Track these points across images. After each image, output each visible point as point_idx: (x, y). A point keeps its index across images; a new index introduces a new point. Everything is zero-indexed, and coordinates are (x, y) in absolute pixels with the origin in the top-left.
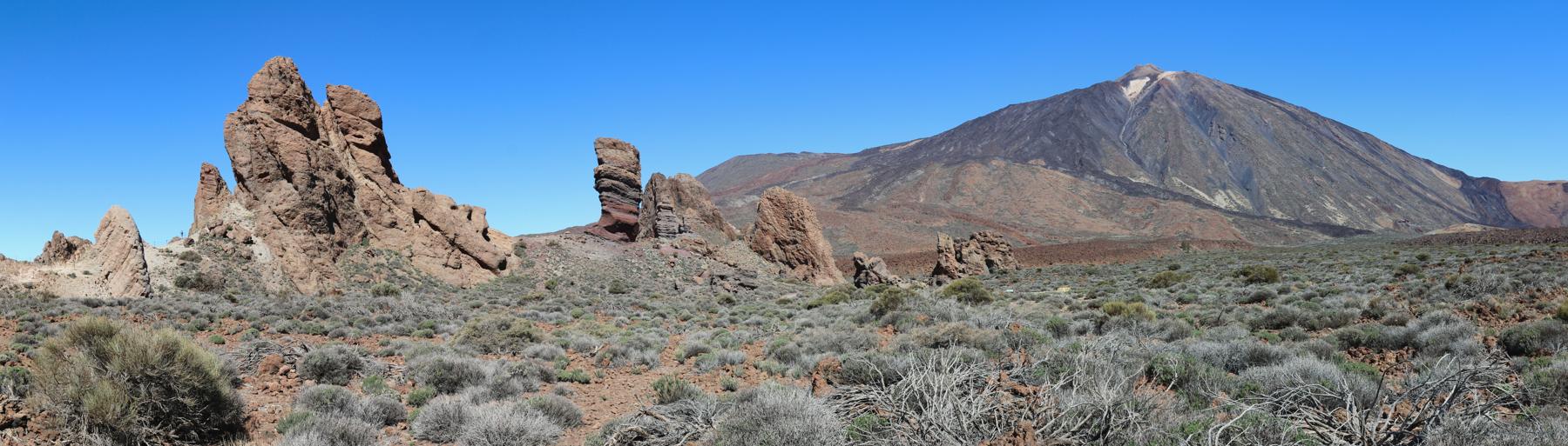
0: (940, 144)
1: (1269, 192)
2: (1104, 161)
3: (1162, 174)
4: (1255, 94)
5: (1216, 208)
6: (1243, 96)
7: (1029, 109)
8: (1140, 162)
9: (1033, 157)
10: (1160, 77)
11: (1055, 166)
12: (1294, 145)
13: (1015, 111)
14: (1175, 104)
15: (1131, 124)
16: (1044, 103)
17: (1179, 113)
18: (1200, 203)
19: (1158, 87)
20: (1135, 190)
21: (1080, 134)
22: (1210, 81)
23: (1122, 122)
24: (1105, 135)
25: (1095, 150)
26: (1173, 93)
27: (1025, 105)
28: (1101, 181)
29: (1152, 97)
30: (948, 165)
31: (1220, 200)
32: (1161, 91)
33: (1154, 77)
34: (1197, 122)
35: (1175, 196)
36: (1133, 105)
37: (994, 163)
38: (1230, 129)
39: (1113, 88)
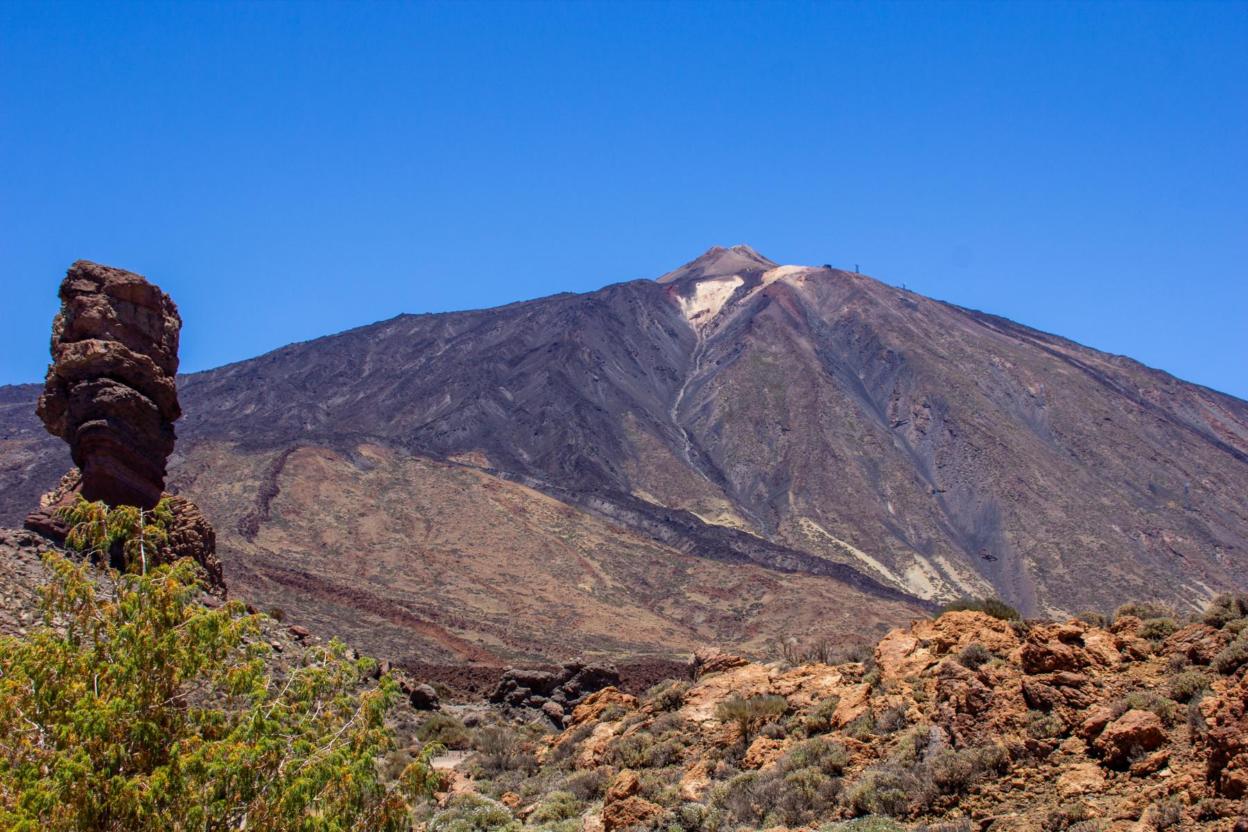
0: (220, 392)
1: (1042, 571)
2: (630, 467)
3: (773, 508)
4: (1002, 324)
5: (913, 600)
6: (972, 330)
7: (450, 330)
8: (719, 477)
9: (458, 448)
10: (770, 277)
11: (518, 472)
12: (1105, 451)
13: (412, 334)
14: (804, 343)
15: (699, 384)
16: (486, 319)
17: (816, 366)
18: (870, 584)
19: (765, 300)
20: (715, 545)
21: (581, 405)
22: (890, 291)
23: (674, 378)
24: (635, 407)
25: (614, 441)
26: (798, 315)
27: (441, 319)
28: (630, 517)
29: (749, 324)
30: (248, 447)
31: (919, 580)
32: (772, 310)
33: (752, 278)
34: (859, 387)
35: (812, 565)
36: (702, 339)
37: (365, 451)
38: (939, 406)
39: (660, 296)
